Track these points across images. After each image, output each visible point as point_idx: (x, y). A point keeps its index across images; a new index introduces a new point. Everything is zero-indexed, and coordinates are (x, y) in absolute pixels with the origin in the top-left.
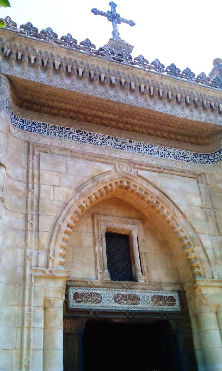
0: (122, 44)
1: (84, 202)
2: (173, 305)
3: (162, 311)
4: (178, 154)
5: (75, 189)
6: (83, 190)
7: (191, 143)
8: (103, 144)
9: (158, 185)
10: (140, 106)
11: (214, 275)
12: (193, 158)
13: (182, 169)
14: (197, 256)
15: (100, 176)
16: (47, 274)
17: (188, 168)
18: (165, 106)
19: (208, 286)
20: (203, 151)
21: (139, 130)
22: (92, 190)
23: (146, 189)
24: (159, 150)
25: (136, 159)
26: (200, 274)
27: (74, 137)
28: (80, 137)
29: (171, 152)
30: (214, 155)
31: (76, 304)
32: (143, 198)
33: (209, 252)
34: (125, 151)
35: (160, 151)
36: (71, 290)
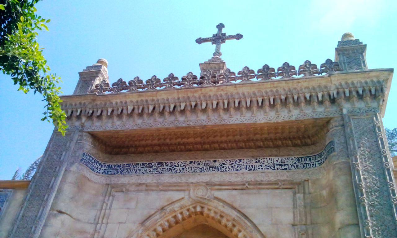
0: (212, 64)
4: (274, 163)
5: (140, 223)
6: (148, 223)
7: (295, 145)
9: (236, 205)
10: (211, 124)
15: (168, 206)
18: (242, 116)
20: (311, 153)
21: (228, 146)
22: (157, 222)
23: (221, 212)
27: (154, 170)
28: (160, 169)
29: (264, 163)
30: (322, 154)
32: (220, 222)
34: (206, 173)
35: (250, 164)
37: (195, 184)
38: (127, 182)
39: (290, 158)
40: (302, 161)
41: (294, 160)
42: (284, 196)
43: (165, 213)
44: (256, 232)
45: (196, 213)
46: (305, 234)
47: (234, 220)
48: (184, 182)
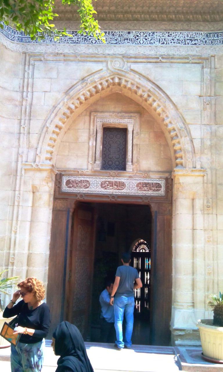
1: (73, 103)
2: (157, 190)
3: (145, 195)
4: (185, 37)
5: (64, 93)
6: (71, 93)
7: (205, 21)
8: (97, 41)
9: (151, 78)
11: (197, 165)
12: (204, 39)
13: (186, 54)
14: (182, 147)
15: (88, 77)
16: (34, 167)
17: (194, 53)
19: (187, 175)
20: (218, 29)
21: (141, 17)
23: (137, 83)
24: (161, 37)
25: (131, 52)
26: (182, 164)
27: (69, 39)
29: (175, 37)
31: (67, 189)
33: (197, 144)
35: (163, 38)
36: (65, 178)
37: (112, 56)
38: (44, 51)
39: (199, 33)
40: (210, 37)
41: (203, 35)
42: (194, 70)
43: (87, 84)
44: (169, 101)
45: (114, 84)
46: (210, 105)
47: (149, 91)
48: (101, 53)
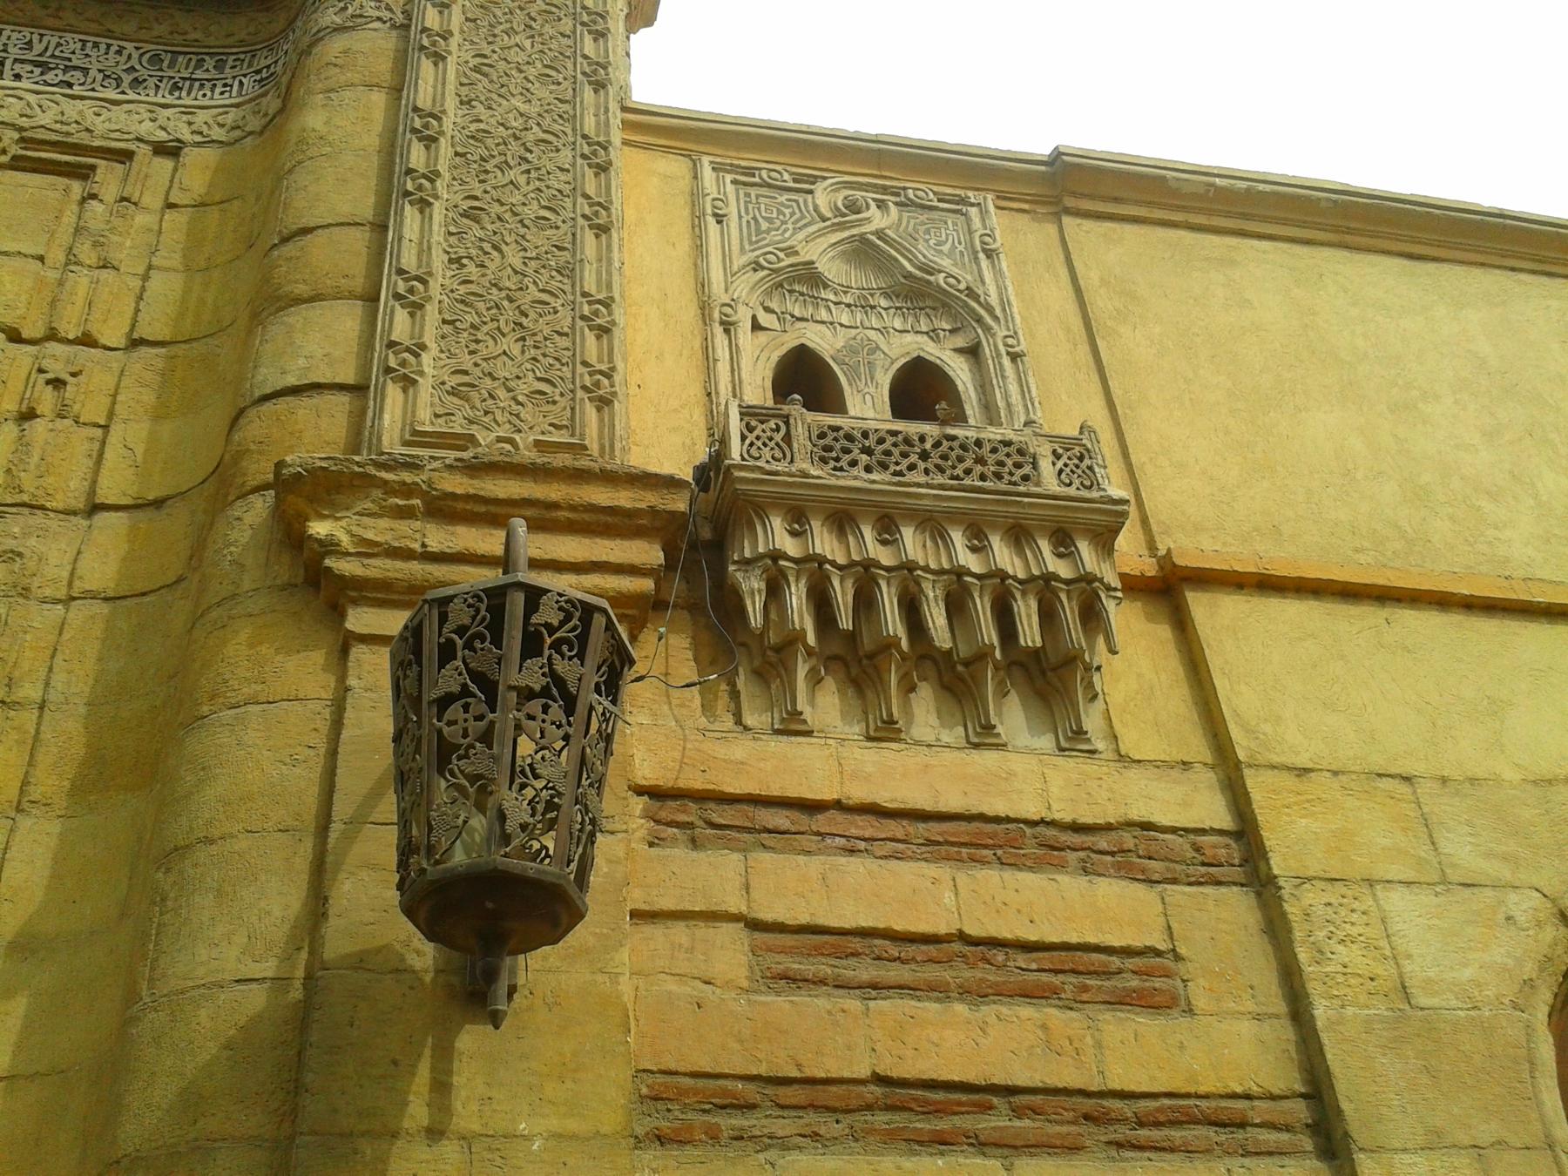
39: (109, 46)
